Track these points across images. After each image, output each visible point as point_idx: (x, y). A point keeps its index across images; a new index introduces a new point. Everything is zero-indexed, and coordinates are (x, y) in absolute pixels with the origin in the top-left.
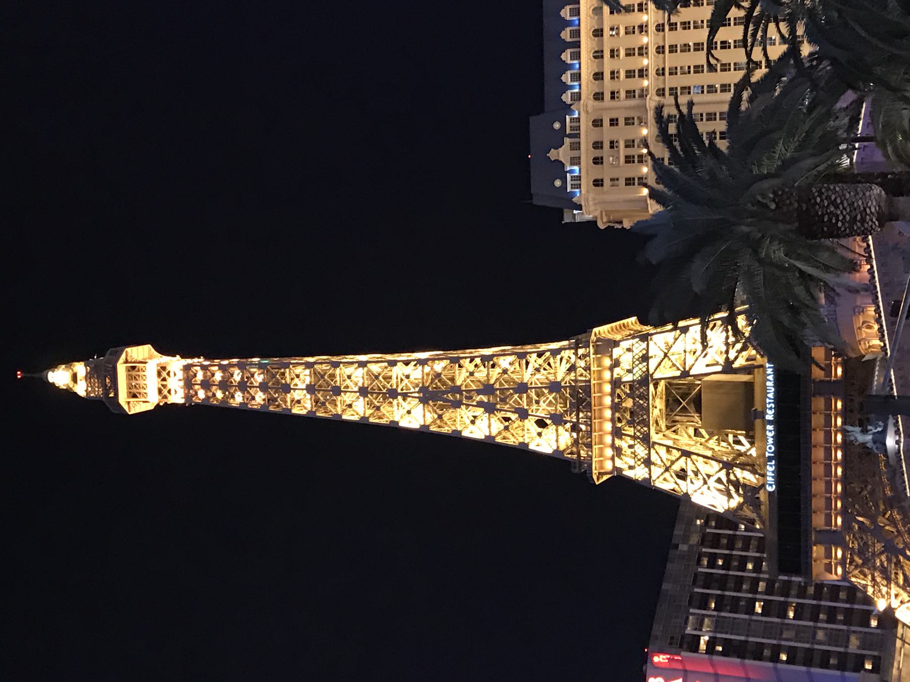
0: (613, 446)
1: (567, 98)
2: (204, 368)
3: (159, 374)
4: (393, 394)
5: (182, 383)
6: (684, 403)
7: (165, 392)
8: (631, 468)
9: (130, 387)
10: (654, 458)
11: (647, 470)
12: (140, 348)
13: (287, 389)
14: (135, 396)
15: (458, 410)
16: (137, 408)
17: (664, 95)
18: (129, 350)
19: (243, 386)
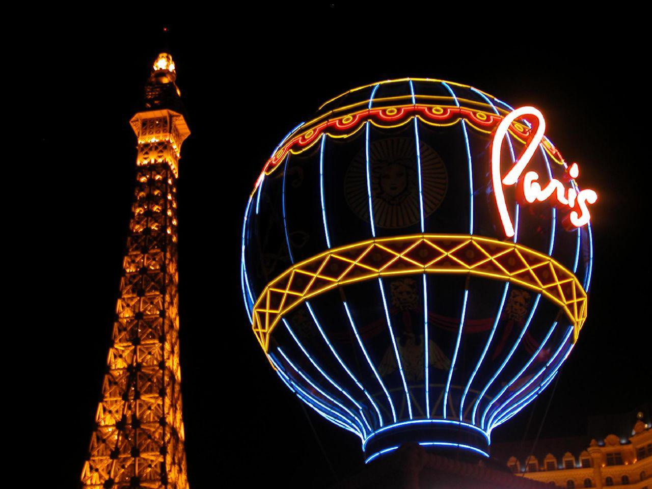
3: (160, 143)
4: (136, 341)
12: (186, 126)
13: (145, 251)
16: (136, 127)
18: (182, 117)
19: (149, 213)
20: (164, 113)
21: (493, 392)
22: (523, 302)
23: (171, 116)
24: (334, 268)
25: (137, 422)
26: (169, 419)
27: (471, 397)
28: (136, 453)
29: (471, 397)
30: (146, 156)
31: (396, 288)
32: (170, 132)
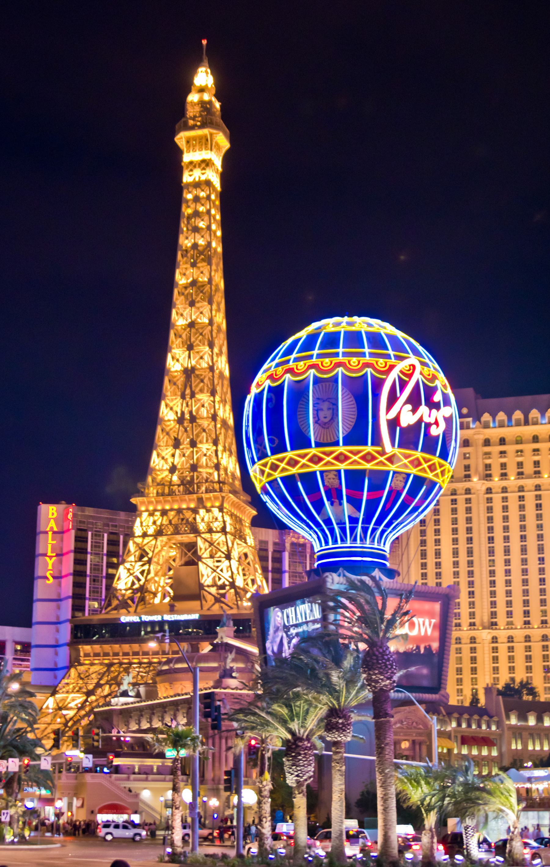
0: (155, 510)
1: (486, 417)
2: (208, 197)
3: (203, 161)
4: (190, 348)
5: (197, 180)
6: (189, 554)
7: (190, 167)
8: (141, 523)
9: (194, 138)
10: (147, 540)
11: (140, 534)
13: (193, 265)
14: (188, 142)
15: (179, 397)
17: (487, 493)
18: (221, 134)
20: (206, 131)
21: (388, 525)
22: (402, 479)
23: (211, 135)
24: (293, 463)
25: (193, 419)
26: (220, 413)
27: (374, 530)
28: (193, 444)
29: (374, 530)
30: (191, 173)
31: (327, 476)
32: (211, 150)
